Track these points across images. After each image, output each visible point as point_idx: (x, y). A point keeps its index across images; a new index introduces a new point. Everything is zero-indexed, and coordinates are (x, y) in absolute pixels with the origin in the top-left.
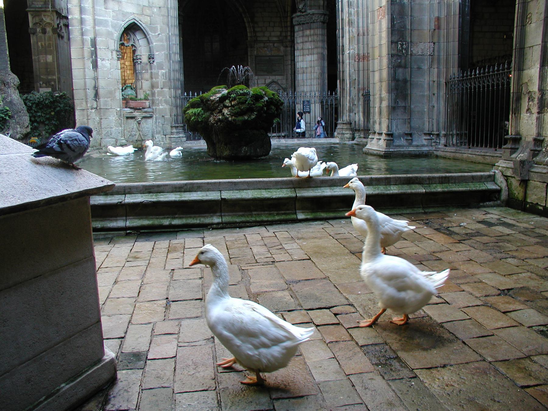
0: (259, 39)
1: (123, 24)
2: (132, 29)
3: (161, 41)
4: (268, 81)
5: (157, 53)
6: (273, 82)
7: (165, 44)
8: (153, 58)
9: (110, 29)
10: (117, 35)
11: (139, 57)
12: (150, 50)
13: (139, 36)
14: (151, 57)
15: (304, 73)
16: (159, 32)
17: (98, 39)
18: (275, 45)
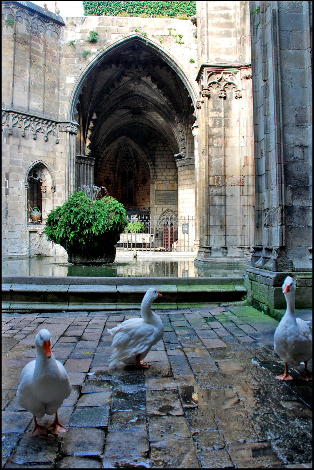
0: (158, 177)
1: (31, 164)
2: (38, 168)
3: (61, 176)
4: (165, 209)
6: (168, 210)
7: (64, 178)
8: (54, 189)
9: (21, 167)
10: (26, 171)
11: (44, 188)
12: (53, 182)
13: (45, 172)
14: (54, 188)
15: (183, 202)
16: (60, 170)
17: (11, 174)
18: (171, 182)
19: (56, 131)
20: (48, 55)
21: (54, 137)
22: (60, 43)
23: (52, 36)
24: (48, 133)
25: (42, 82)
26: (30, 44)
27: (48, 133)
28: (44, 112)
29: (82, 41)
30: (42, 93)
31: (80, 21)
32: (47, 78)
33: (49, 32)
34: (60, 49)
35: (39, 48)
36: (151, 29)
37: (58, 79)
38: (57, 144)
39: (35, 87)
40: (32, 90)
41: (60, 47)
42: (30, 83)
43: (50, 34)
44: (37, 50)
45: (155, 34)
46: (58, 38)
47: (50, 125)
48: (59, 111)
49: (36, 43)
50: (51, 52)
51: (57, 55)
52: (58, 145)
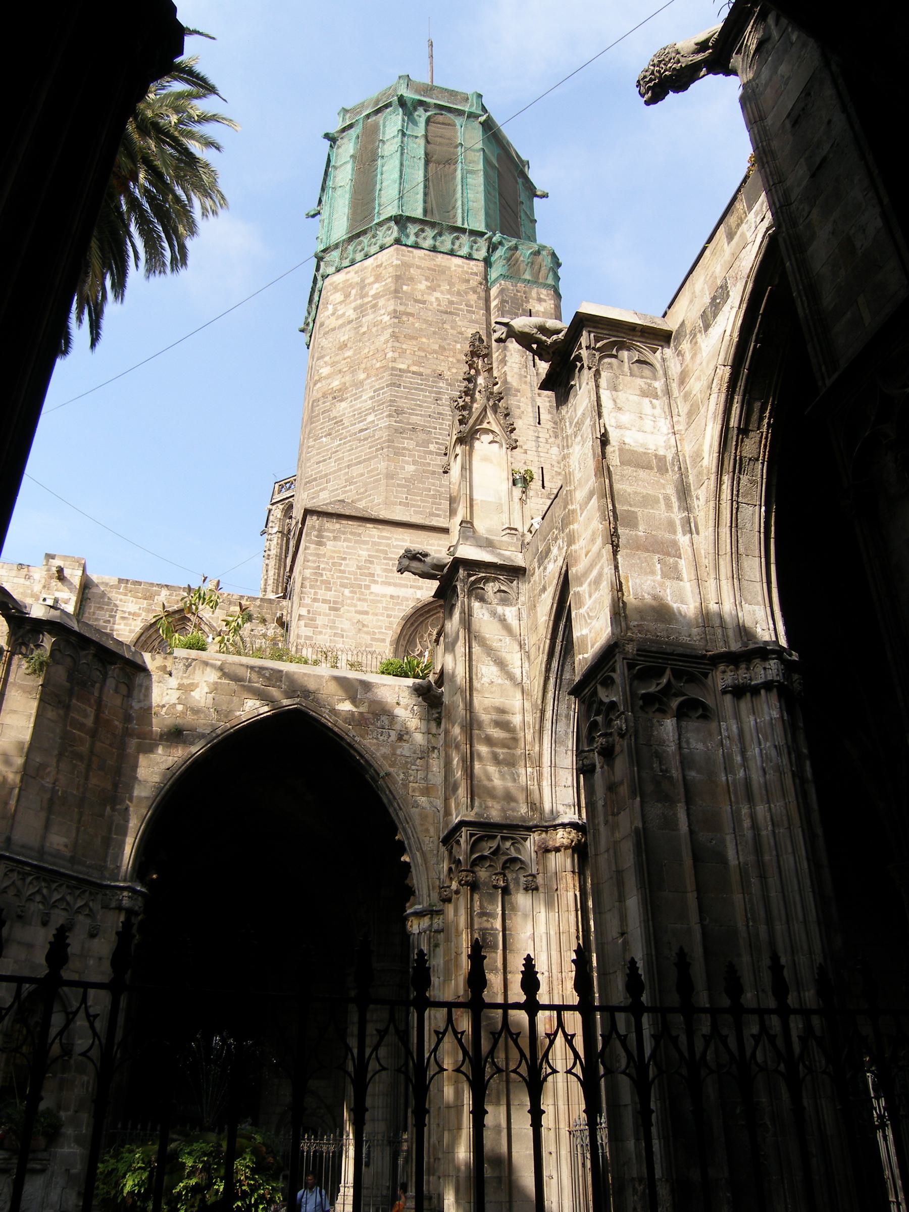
5: (79, 1042)
19: (96, 906)
21: (88, 921)
22: (131, 707)
23: (116, 691)
24: (78, 911)
27: (78, 911)
28: (72, 860)
29: (180, 708)
31: (181, 666)
32: (93, 781)
33: (111, 683)
35: (86, 716)
37: (115, 786)
38: (92, 936)
41: (130, 715)
42: (54, 791)
43: (113, 686)
44: (82, 720)
46: (129, 695)
47: (84, 892)
48: (109, 859)
49: (83, 706)
52: (96, 940)
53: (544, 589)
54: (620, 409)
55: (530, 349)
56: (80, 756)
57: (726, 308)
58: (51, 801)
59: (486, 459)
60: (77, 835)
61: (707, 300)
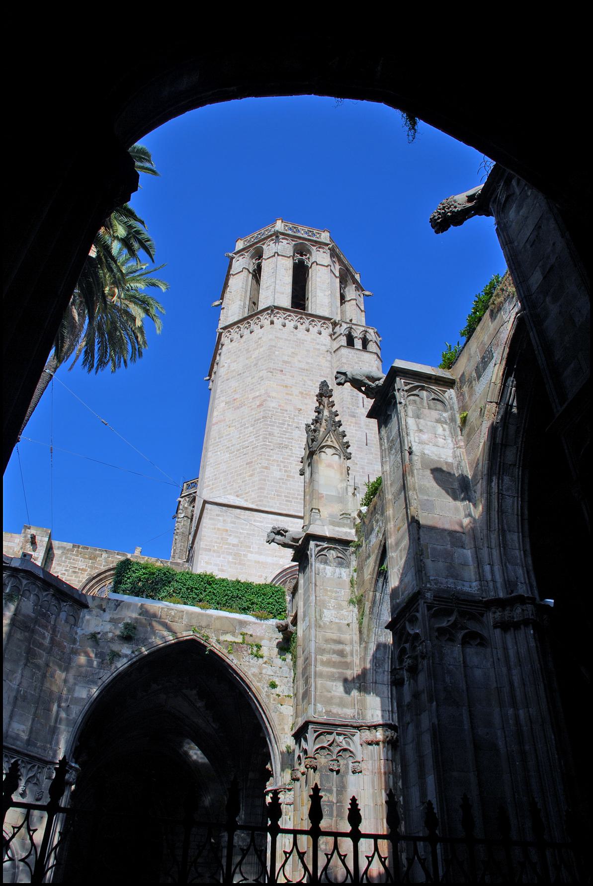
20: (55, 649)
22: (76, 633)
23: (67, 621)
25: (37, 690)
26: (33, 631)
29: (110, 635)
30: (33, 710)
31: (113, 605)
33: (63, 615)
34: (74, 641)
35: (44, 638)
36: (217, 631)
39: (24, 698)
40: (19, 703)
41: (75, 639)
42: (18, 691)
43: (64, 618)
44: (41, 640)
45: (222, 638)
46: (75, 624)
49: (42, 630)
50: (60, 646)
51: (67, 650)
53: (369, 556)
54: (421, 431)
55: (361, 391)
56: (38, 667)
57: (491, 364)
58: (16, 698)
59: (329, 466)
60: (32, 724)
61: (478, 359)
